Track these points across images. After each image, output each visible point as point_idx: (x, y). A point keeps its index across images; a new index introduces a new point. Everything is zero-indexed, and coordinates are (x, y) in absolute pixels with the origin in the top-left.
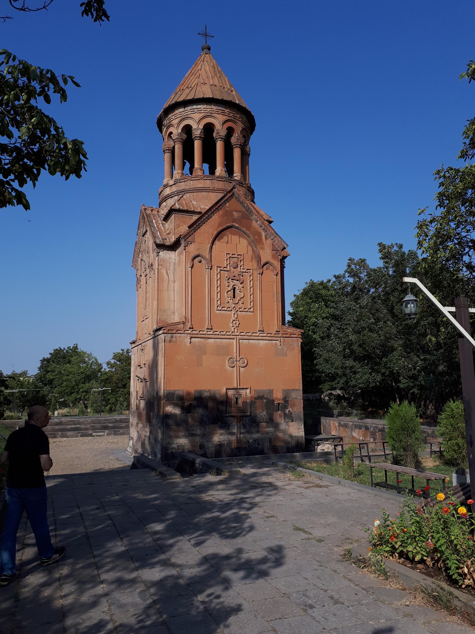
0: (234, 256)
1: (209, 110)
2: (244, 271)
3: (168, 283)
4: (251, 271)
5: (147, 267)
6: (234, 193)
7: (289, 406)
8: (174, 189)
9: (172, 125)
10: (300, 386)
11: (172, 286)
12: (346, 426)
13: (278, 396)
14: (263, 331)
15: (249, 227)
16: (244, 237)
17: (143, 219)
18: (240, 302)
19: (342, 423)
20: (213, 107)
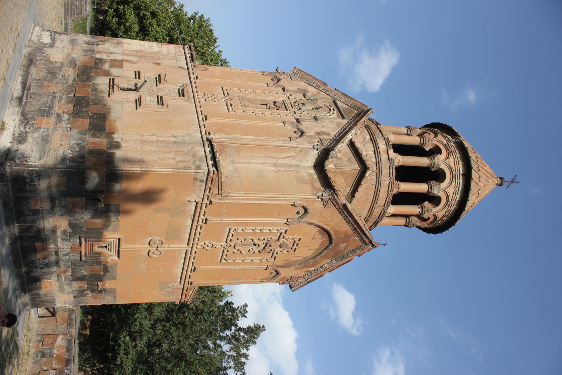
0: (296, 244)
2: (275, 254)
3: (275, 158)
4: (272, 260)
6: (367, 245)
7: (93, 294)
8: (384, 157)
9: (448, 157)
10: (119, 302)
11: (269, 162)
12: (70, 323)
13: (108, 284)
14: (194, 270)
15: (325, 257)
18: (236, 251)
19: (74, 317)
20: (455, 206)
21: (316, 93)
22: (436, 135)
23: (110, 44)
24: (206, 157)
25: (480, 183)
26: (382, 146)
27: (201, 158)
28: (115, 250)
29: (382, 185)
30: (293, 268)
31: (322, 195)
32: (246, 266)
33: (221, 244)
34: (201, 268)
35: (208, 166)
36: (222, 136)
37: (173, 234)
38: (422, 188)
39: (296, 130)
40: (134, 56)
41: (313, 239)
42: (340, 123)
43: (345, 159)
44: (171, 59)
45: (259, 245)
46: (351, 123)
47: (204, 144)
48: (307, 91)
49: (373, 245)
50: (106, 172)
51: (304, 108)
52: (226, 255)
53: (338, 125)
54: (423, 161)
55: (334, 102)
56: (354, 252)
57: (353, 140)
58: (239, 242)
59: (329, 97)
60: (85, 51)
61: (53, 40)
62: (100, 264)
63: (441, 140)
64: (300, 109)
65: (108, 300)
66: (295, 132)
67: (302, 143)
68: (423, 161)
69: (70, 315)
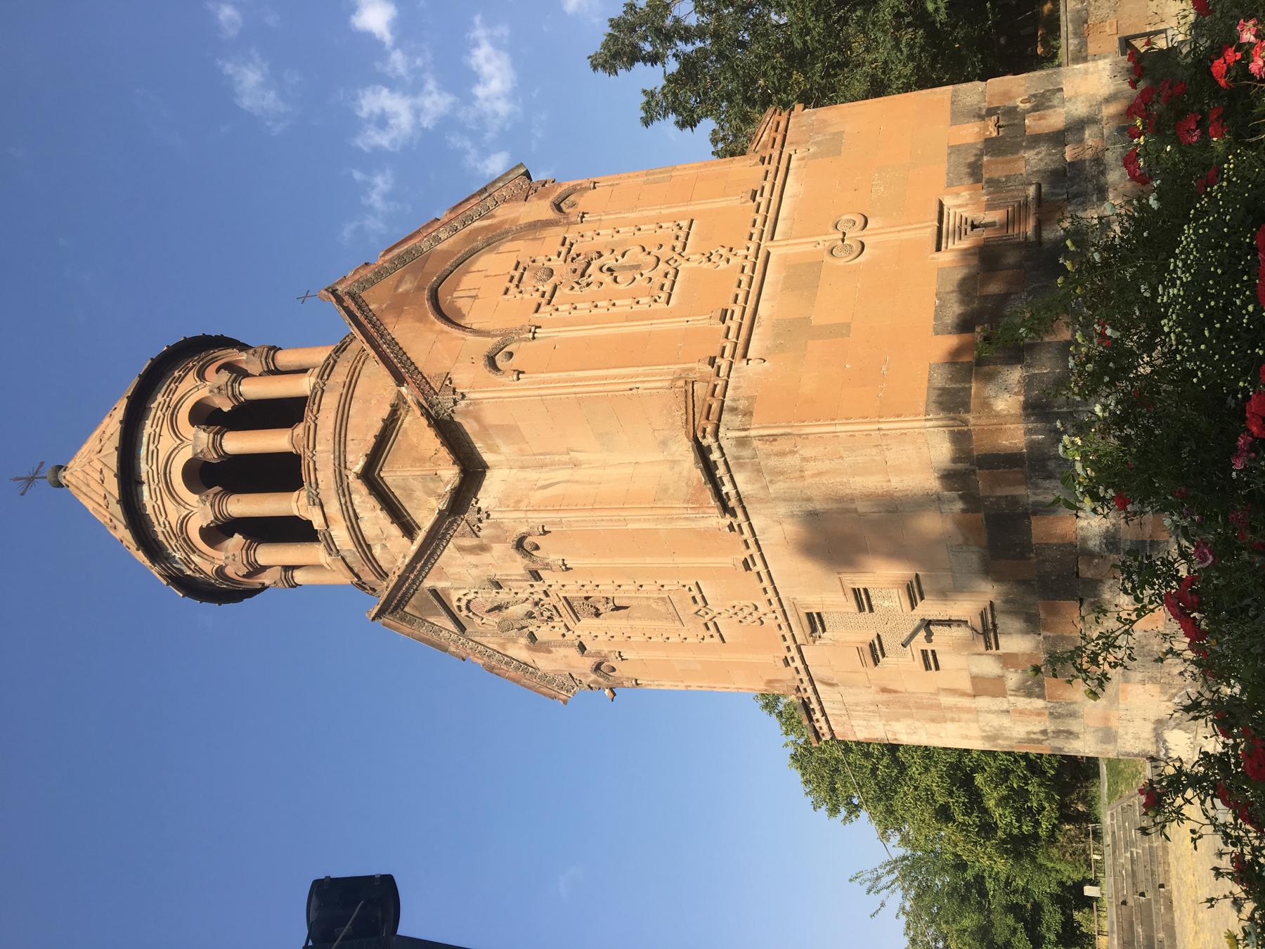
0: (516, 279)
1: (159, 413)
2: (564, 250)
3: (577, 482)
5: (539, 587)
6: (348, 293)
8: (333, 508)
9: (183, 523)
10: (944, 93)
13: (971, 133)
15: (447, 254)
16: (471, 264)
17: (411, 623)
18: (655, 251)
19: (1073, 42)
20: (154, 405)
21: (509, 645)
22: (220, 571)
23: (1015, 734)
24: (729, 470)
25: (99, 466)
26: (341, 534)
27: (741, 466)
28: (950, 222)
29: (331, 442)
30: (523, 221)
31: (455, 402)
32: (632, 215)
33: (689, 265)
34: (737, 202)
35: (720, 448)
36: (702, 524)
37: (806, 277)
38: (238, 443)
39: (535, 553)
40: (950, 708)
41: (475, 297)
42: (439, 579)
43: (419, 494)
44: (857, 705)
45: (601, 269)
46: (414, 582)
47: (740, 501)
48: (529, 648)
49: (334, 292)
50: (968, 411)
51: (528, 606)
52: (677, 238)
53: (442, 575)
54: (242, 506)
55: (462, 629)
56: (380, 274)
57: (406, 540)
58: (647, 274)
59: (477, 639)
60: (1073, 715)
61: (1159, 738)
62: (990, 182)
63: (206, 561)
64: (536, 604)
65: (973, 92)
66: (537, 548)
67: (516, 522)
68: (242, 506)
69: (1083, 44)
